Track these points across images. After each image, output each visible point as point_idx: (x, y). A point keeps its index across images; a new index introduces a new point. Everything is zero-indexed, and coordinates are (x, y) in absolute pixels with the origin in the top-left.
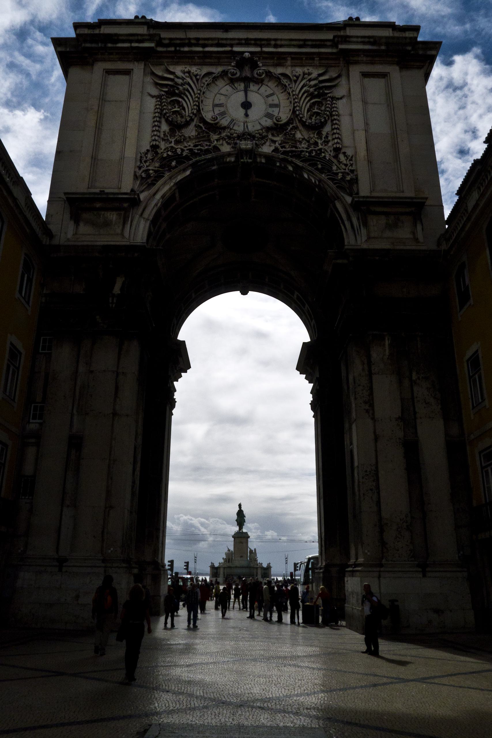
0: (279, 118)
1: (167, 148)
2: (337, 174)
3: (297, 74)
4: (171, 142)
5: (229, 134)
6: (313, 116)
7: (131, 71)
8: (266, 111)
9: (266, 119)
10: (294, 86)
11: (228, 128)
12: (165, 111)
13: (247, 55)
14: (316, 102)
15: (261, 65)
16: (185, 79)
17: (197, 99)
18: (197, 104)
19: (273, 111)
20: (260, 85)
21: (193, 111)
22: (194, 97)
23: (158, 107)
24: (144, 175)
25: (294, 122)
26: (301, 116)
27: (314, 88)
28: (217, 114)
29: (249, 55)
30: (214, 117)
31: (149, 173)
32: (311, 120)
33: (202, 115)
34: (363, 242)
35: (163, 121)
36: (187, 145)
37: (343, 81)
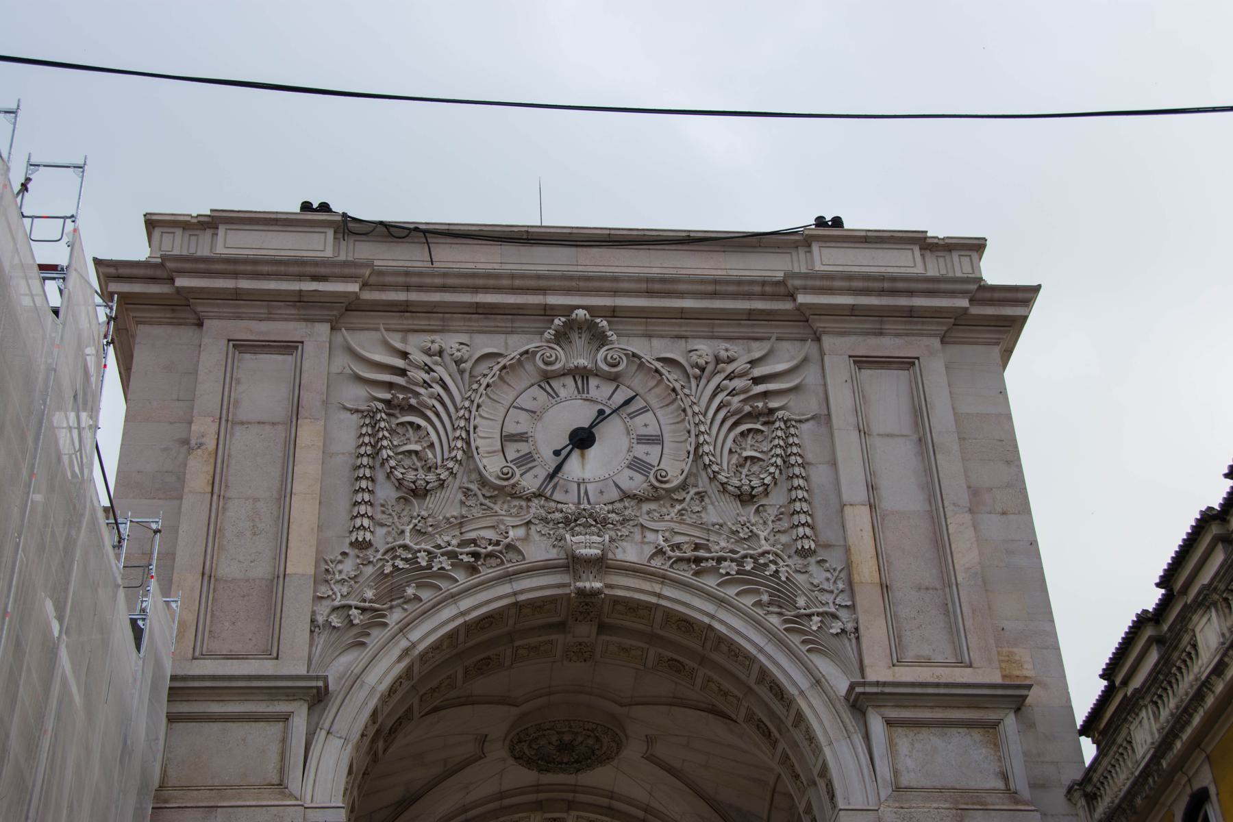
0: (664, 473)
1: (393, 549)
2: (809, 616)
3: (701, 362)
4: (403, 532)
5: (542, 512)
6: (742, 466)
7: (297, 348)
8: (630, 453)
9: (632, 473)
10: (693, 393)
11: (540, 495)
12: (384, 453)
13: (581, 313)
14: (749, 430)
15: (615, 337)
16: (434, 371)
17: (462, 423)
18: (464, 435)
19: (647, 454)
20: (615, 385)
21: (453, 454)
22: (454, 418)
23: (367, 440)
24: (336, 621)
25: (700, 483)
26: (715, 468)
27: (742, 397)
28: (512, 461)
29: (585, 315)
30: (505, 470)
31: (349, 616)
32: (740, 481)
33: (475, 462)
34: (883, 798)
35: (380, 476)
36: (443, 544)
37: (810, 376)
